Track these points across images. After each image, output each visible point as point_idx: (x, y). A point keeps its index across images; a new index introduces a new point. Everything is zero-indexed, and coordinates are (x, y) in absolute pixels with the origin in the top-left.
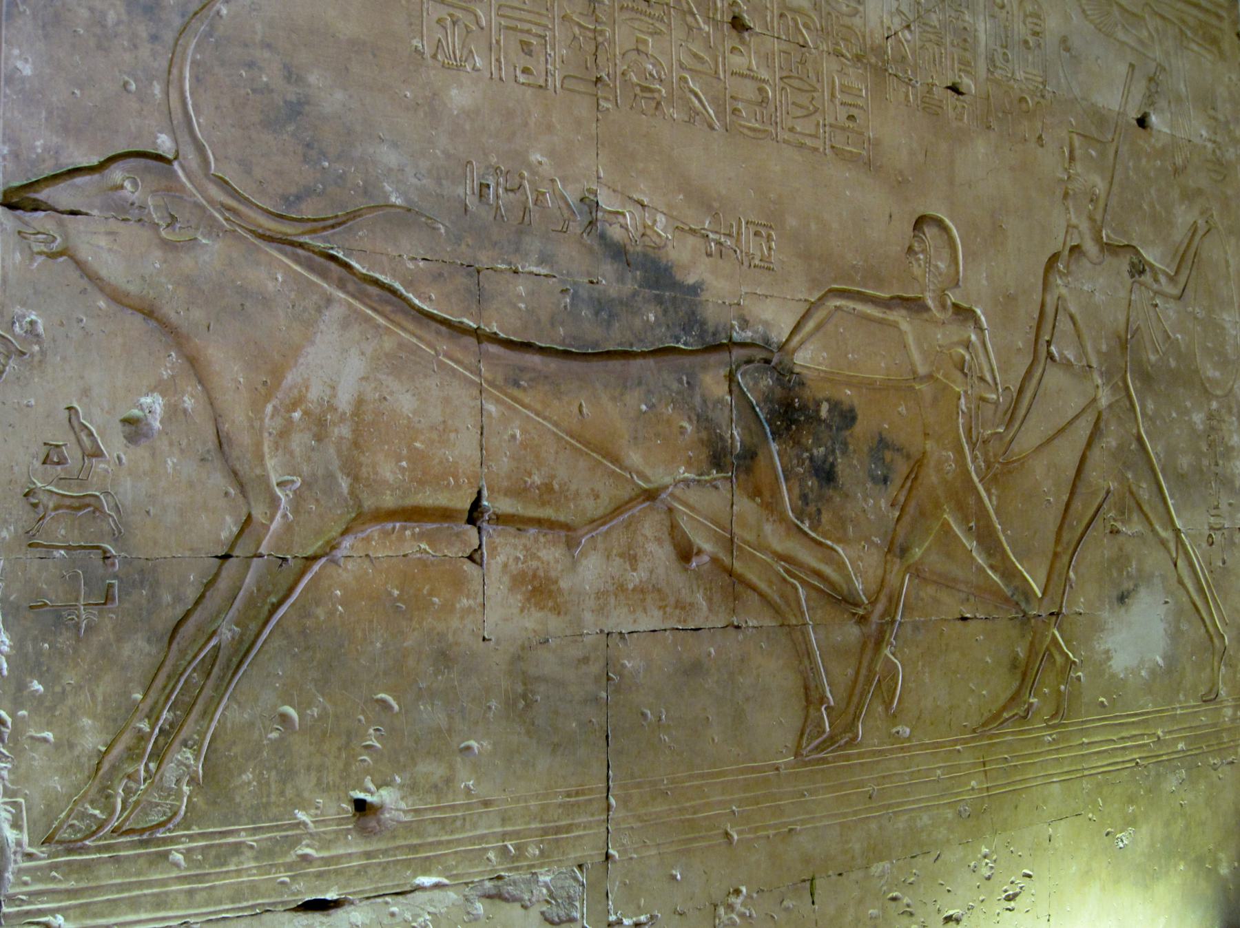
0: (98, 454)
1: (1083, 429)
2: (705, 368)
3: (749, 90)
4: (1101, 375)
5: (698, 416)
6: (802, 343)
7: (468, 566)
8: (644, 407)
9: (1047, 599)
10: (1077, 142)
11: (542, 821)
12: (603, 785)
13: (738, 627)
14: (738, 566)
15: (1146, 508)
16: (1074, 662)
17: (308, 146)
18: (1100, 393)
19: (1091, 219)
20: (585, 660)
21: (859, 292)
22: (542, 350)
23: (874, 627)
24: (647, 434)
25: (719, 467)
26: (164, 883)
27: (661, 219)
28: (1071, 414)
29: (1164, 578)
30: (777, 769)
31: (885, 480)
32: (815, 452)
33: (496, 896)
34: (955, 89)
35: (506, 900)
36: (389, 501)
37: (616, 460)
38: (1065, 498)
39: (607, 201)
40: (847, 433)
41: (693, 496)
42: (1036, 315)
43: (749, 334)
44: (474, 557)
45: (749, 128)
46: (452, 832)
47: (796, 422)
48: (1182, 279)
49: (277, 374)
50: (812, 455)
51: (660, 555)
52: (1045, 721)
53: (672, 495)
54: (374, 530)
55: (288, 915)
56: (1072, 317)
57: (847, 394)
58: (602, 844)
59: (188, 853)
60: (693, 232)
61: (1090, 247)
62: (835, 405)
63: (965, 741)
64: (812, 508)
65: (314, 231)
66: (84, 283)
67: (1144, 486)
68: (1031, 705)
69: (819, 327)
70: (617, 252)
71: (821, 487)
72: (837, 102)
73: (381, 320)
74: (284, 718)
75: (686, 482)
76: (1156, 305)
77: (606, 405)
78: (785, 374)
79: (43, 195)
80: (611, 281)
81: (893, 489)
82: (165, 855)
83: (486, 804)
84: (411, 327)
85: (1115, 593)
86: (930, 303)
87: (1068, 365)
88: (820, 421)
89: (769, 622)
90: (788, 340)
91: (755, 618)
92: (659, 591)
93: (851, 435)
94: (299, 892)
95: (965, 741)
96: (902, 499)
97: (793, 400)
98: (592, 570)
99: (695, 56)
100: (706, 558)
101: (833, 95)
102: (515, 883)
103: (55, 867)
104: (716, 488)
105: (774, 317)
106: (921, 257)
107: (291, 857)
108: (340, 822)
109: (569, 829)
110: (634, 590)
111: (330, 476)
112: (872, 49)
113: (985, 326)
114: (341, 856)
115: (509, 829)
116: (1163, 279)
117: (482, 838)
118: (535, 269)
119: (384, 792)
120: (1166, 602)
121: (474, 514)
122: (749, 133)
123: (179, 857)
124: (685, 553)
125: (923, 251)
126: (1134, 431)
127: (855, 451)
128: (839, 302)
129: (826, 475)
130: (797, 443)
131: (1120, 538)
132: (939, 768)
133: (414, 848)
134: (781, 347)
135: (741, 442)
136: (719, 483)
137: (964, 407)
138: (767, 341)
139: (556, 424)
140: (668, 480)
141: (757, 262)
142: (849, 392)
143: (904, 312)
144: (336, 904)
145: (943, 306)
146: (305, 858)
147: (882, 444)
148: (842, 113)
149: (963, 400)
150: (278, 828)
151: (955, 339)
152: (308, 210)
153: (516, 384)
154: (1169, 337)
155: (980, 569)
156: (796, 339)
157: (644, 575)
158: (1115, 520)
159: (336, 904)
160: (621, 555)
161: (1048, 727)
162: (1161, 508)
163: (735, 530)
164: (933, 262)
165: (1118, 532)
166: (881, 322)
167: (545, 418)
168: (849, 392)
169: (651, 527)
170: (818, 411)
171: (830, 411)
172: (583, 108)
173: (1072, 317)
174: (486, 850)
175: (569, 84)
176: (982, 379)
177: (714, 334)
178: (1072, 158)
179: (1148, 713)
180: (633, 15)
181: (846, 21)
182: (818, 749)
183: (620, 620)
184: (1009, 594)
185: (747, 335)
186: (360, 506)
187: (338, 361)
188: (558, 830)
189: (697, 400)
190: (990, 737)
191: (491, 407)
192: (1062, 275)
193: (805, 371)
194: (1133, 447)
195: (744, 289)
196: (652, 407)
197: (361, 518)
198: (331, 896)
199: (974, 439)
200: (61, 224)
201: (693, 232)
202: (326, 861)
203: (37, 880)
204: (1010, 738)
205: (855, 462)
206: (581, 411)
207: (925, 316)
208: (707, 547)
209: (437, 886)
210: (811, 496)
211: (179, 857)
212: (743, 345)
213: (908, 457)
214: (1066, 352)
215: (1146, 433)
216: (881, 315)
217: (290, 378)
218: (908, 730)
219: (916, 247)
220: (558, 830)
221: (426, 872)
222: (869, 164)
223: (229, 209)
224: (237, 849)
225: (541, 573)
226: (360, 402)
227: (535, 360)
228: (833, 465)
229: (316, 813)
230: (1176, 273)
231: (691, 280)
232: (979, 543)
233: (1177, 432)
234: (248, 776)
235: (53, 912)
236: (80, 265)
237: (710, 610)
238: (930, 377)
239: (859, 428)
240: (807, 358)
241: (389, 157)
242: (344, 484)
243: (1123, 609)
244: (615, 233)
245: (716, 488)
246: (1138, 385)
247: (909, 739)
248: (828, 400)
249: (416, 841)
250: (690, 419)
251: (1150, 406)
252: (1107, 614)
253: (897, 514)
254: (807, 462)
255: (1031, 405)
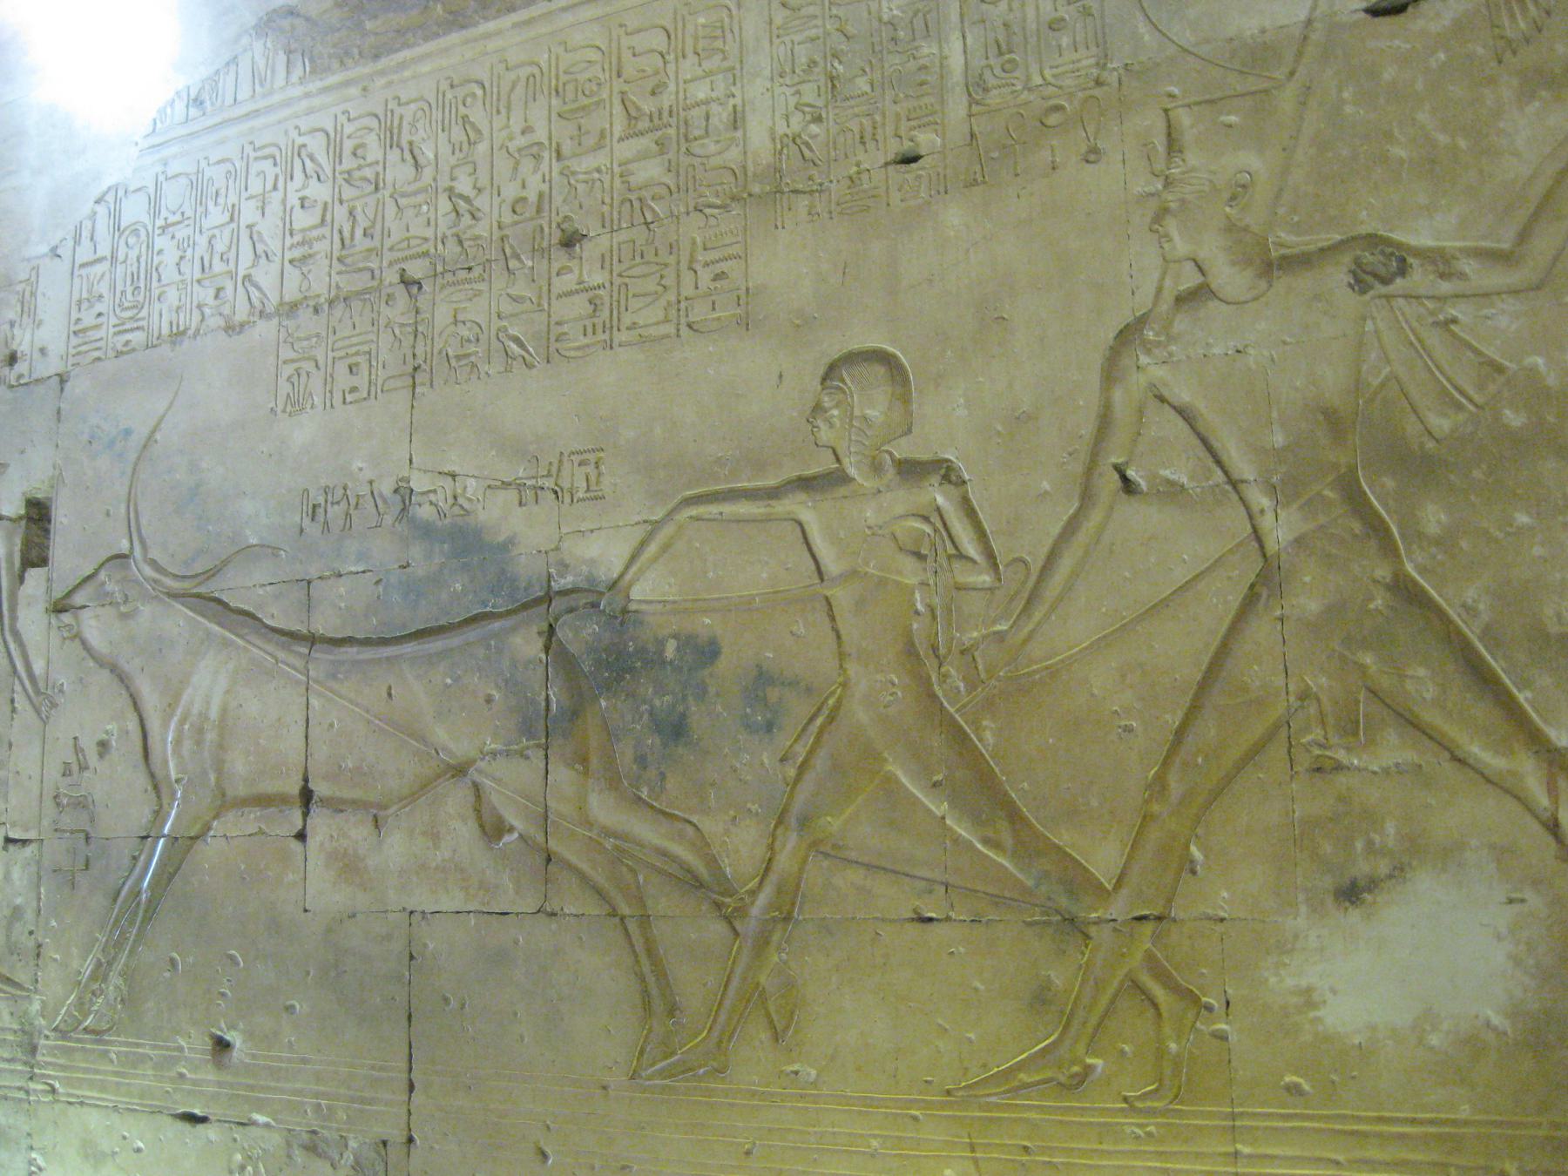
0: (87, 768)
1: (1224, 596)
2: (514, 629)
3: (580, 305)
4: (1272, 490)
5: (506, 681)
6: (641, 571)
7: (296, 845)
8: (449, 681)
9: (1124, 892)
10: (1184, 118)
11: (349, 1088)
12: (404, 1065)
13: (553, 914)
14: (553, 844)
15: (1430, 717)
16: (1209, 1008)
17: (200, 518)
18: (1267, 522)
19: (1230, 228)
20: (388, 937)
21: (731, 490)
22: (367, 642)
23: (753, 922)
24: (458, 709)
25: (531, 735)
26: (105, 1072)
27: (471, 483)
28: (1181, 575)
29: (1503, 854)
30: (605, 1088)
31: (769, 727)
32: (657, 703)
33: (312, 1149)
34: (910, 159)
35: (319, 1156)
36: (242, 791)
37: (423, 739)
38: (1174, 719)
39: (419, 483)
40: (706, 672)
41: (500, 767)
42: (1088, 430)
43: (570, 579)
44: (301, 836)
45: (578, 348)
46: (278, 1080)
47: (631, 670)
48: (1543, 245)
49: (177, 697)
50: (652, 707)
51: (462, 833)
52: (1125, 1099)
53: (480, 771)
54: (230, 816)
55: (169, 1120)
56: (1184, 413)
57: (706, 624)
58: (403, 1125)
59: (118, 1054)
60: (506, 485)
61: (1229, 277)
62: (687, 642)
63: (928, 1105)
64: (652, 773)
65: (200, 584)
66: (84, 654)
67: (1422, 672)
68: (1089, 1069)
69: (665, 548)
70: (426, 531)
71: (665, 745)
72: (698, 267)
73: (240, 642)
74: (173, 962)
75: (494, 754)
76: (1454, 321)
77: (415, 686)
78: (624, 617)
79: (68, 601)
80: (422, 559)
81: (783, 740)
82: (107, 1052)
83: (304, 1061)
84: (258, 642)
85: (1328, 882)
86: (852, 472)
87: (1172, 492)
88: (663, 663)
89: (593, 908)
90: (622, 576)
91: (573, 902)
92: (462, 870)
93: (711, 675)
94: (175, 1102)
95: (928, 1105)
96: (801, 751)
97: (626, 645)
98: (397, 847)
99: (515, 299)
100: (516, 835)
101: (692, 260)
102: (326, 1141)
103: (56, 1047)
104: (527, 758)
105: (601, 551)
106: (835, 412)
107: (173, 1074)
108: (203, 1052)
109: (371, 1101)
110: (437, 868)
111: (205, 773)
112: (755, 175)
113: (967, 477)
114: (203, 1080)
115: (322, 1088)
116: (1468, 266)
117: (299, 1092)
118: (353, 569)
119: (234, 1033)
120: (1511, 901)
121: (307, 796)
122: (579, 354)
123: (114, 1056)
124: (492, 830)
125: (837, 406)
126: (1383, 572)
127: (718, 694)
128: (694, 511)
129: (675, 730)
130: (631, 695)
131: (1342, 779)
132: (875, 1136)
133: (252, 1088)
134: (613, 585)
135: (558, 702)
136: (529, 752)
137: (920, 607)
138: (591, 579)
139: (368, 711)
140: (473, 753)
141: (581, 495)
142: (707, 621)
143: (802, 496)
144: (203, 1120)
145: (876, 468)
146: (182, 1076)
147: (762, 680)
148: (705, 276)
149: (917, 596)
150: (168, 1048)
151: (900, 509)
152: (198, 568)
153: (334, 677)
154: (1500, 369)
155: (957, 840)
156: (634, 569)
157: (447, 854)
158: (1321, 746)
159: (203, 1120)
160: (424, 833)
161: (1133, 1109)
162: (1483, 711)
163: (552, 803)
164: (857, 412)
165: (1339, 767)
166: (768, 519)
167: (357, 705)
168: (707, 621)
169: (456, 799)
170: (661, 652)
171: (678, 649)
172: (401, 400)
173: (1184, 413)
174: (303, 1103)
175: (391, 384)
176: (961, 556)
177: (526, 589)
178: (1173, 145)
179: (1454, 1123)
180: (451, 289)
181: (716, 161)
182: (662, 1074)
183: (422, 899)
184: (1030, 883)
185: (567, 581)
186: (224, 795)
187: (212, 679)
188: (363, 1101)
189: (506, 663)
190: (988, 1107)
191: (314, 702)
192: (1148, 348)
193: (644, 607)
194: (1378, 603)
195: (564, 531)
196: (457, 679)
197: (225, 804)
198: (197, 1112)
199: (942, 651)
200: (76, 617)
201: (506, 485)
202: (195, 1082)
203: (49, 1054)
204: (1033, 1115)
205: (719, 708)
206: (390, 695)
207: (843, 491)
208: (516, 823)
209: (267, 1125)
210: (650, 758)
211: (114, 1056)
212: (564, 593)
213: (809, 690)
214: (1166, 473)
215: (1423, 570)
216: (762, 510)
217: (185, 698)
218: (814, 1072)
219: (827, 401)
220: (363, 1101)
221: (260, 1111)
222: (745, 323)
223: (155, 581)
224: (143, 1058)
225: (351, 851)
226: (224, 711)
227: (351, 652)
228: (683, 716)
229: (194, 1044)
230: (1523, 236)
231: (501, 539)
232: (953, 805)
233: (1537, 551)
234: (151, 1004)
235: (56, 1078)
236: (84, 643)
237: (517, 893)
238: (853, 574)
239: (722, 664)
240: (645, 590)
241: (248, 506)
242: (213, 777)
243: (1355, 915)
244: (425, 512)
245: (527, 758)
246: (1390, 483)
247: (814, 1084)
248: (675, 636)
249: (251, 1082)
250: (498, 687)
251: (1434, 517)
252: (1301, 922)
253: (792, 772)
254: (646, 716)
255: (1075, 575)
